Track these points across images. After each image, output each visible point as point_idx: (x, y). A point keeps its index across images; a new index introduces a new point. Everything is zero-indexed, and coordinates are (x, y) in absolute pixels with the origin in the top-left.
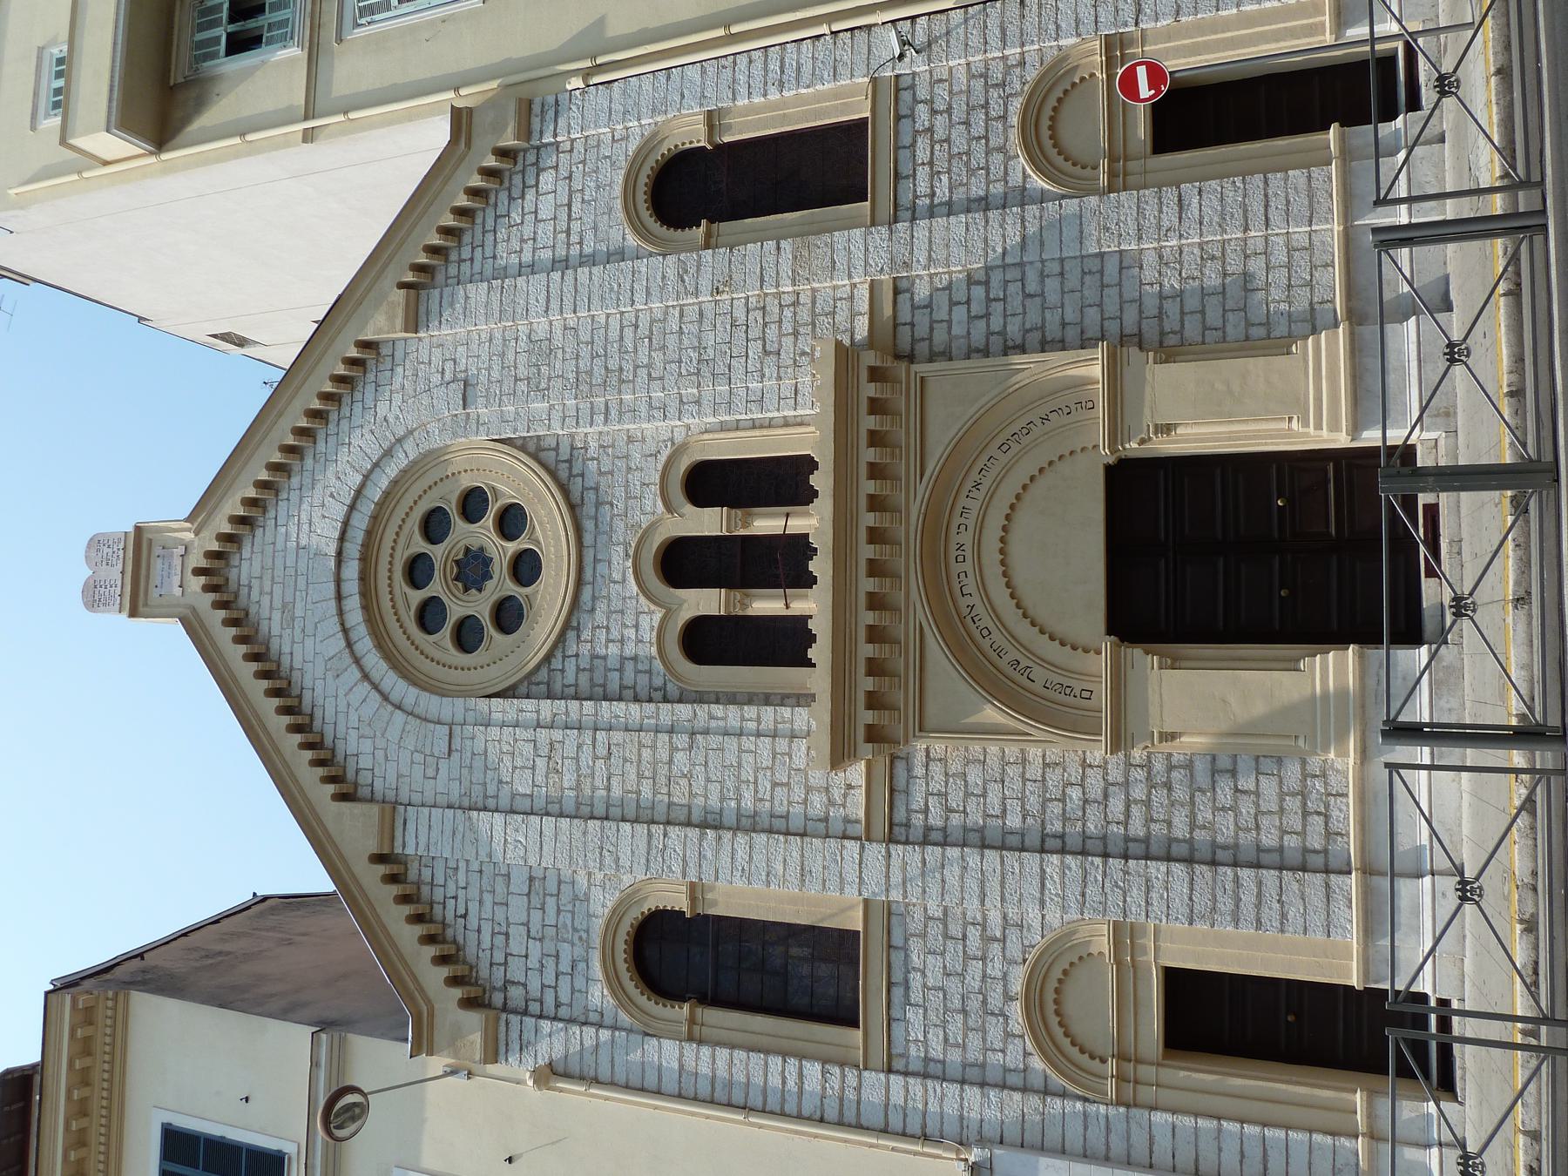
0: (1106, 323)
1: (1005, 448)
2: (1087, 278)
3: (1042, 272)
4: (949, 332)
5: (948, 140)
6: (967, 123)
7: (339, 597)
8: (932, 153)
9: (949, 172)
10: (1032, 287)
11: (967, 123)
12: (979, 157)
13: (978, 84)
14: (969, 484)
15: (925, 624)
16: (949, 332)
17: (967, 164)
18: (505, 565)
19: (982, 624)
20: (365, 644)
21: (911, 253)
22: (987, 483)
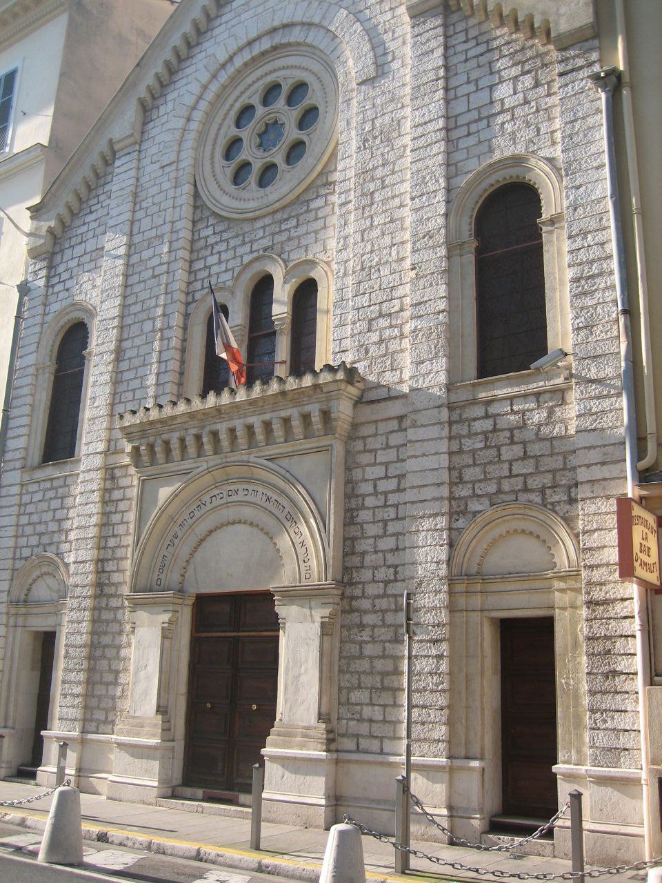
0: (360, 586)
1: (289, 517)
2: (392, 570)
3: (400, 534)
4: (368, 465)
5: (512, 442)
6: (525, 456)
7: (250, 43)
8: (503, 430)
9: (486, 447)
10: (391, 528)
11: (525, 456)
12: (494, 470)
13: (557, 463)
14: (270, 494)
15: (190, 476)
16: (368, 465)
17: (490, 463)
18: (268, 159)
19: (196, 512)
20: (223, 77)
21: (422, 426)
22: (270, 506)
